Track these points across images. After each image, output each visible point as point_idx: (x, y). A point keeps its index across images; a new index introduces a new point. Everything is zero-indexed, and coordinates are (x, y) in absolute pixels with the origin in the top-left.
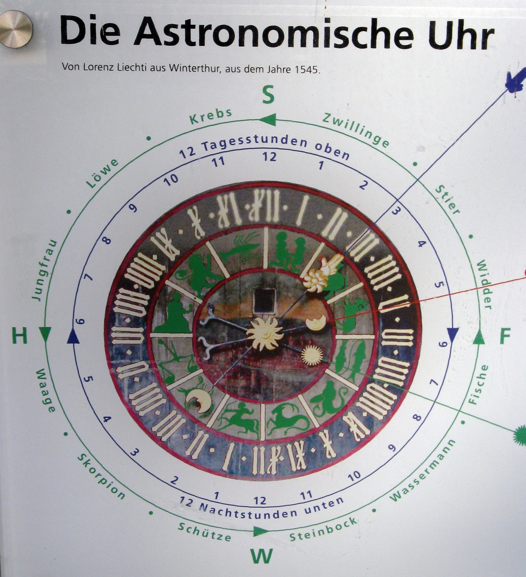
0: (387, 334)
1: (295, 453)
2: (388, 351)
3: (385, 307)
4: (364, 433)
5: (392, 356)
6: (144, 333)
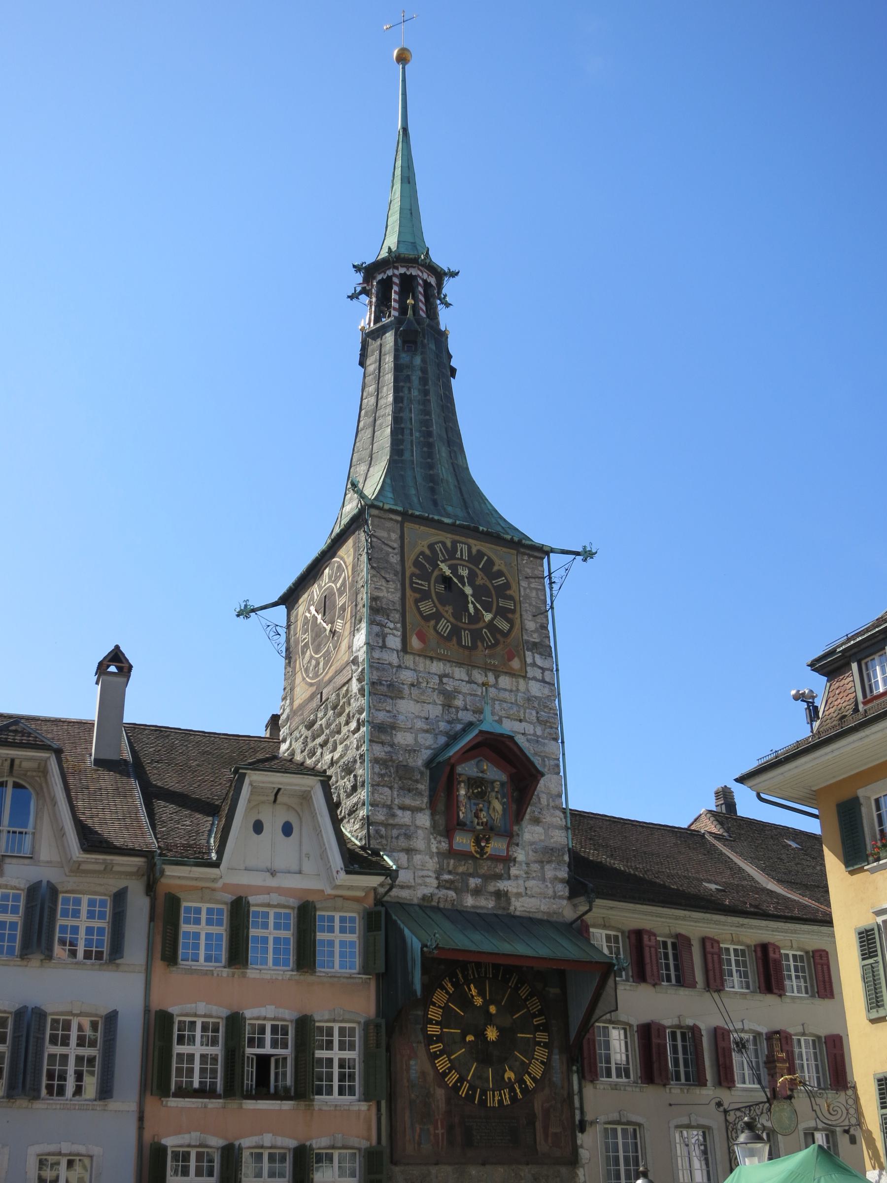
0: (538, 1035)
1: (505, 1095)
2: (539, 1044)
3: (536, 1021)
4: (532, 1085)
5: (541, 1046)
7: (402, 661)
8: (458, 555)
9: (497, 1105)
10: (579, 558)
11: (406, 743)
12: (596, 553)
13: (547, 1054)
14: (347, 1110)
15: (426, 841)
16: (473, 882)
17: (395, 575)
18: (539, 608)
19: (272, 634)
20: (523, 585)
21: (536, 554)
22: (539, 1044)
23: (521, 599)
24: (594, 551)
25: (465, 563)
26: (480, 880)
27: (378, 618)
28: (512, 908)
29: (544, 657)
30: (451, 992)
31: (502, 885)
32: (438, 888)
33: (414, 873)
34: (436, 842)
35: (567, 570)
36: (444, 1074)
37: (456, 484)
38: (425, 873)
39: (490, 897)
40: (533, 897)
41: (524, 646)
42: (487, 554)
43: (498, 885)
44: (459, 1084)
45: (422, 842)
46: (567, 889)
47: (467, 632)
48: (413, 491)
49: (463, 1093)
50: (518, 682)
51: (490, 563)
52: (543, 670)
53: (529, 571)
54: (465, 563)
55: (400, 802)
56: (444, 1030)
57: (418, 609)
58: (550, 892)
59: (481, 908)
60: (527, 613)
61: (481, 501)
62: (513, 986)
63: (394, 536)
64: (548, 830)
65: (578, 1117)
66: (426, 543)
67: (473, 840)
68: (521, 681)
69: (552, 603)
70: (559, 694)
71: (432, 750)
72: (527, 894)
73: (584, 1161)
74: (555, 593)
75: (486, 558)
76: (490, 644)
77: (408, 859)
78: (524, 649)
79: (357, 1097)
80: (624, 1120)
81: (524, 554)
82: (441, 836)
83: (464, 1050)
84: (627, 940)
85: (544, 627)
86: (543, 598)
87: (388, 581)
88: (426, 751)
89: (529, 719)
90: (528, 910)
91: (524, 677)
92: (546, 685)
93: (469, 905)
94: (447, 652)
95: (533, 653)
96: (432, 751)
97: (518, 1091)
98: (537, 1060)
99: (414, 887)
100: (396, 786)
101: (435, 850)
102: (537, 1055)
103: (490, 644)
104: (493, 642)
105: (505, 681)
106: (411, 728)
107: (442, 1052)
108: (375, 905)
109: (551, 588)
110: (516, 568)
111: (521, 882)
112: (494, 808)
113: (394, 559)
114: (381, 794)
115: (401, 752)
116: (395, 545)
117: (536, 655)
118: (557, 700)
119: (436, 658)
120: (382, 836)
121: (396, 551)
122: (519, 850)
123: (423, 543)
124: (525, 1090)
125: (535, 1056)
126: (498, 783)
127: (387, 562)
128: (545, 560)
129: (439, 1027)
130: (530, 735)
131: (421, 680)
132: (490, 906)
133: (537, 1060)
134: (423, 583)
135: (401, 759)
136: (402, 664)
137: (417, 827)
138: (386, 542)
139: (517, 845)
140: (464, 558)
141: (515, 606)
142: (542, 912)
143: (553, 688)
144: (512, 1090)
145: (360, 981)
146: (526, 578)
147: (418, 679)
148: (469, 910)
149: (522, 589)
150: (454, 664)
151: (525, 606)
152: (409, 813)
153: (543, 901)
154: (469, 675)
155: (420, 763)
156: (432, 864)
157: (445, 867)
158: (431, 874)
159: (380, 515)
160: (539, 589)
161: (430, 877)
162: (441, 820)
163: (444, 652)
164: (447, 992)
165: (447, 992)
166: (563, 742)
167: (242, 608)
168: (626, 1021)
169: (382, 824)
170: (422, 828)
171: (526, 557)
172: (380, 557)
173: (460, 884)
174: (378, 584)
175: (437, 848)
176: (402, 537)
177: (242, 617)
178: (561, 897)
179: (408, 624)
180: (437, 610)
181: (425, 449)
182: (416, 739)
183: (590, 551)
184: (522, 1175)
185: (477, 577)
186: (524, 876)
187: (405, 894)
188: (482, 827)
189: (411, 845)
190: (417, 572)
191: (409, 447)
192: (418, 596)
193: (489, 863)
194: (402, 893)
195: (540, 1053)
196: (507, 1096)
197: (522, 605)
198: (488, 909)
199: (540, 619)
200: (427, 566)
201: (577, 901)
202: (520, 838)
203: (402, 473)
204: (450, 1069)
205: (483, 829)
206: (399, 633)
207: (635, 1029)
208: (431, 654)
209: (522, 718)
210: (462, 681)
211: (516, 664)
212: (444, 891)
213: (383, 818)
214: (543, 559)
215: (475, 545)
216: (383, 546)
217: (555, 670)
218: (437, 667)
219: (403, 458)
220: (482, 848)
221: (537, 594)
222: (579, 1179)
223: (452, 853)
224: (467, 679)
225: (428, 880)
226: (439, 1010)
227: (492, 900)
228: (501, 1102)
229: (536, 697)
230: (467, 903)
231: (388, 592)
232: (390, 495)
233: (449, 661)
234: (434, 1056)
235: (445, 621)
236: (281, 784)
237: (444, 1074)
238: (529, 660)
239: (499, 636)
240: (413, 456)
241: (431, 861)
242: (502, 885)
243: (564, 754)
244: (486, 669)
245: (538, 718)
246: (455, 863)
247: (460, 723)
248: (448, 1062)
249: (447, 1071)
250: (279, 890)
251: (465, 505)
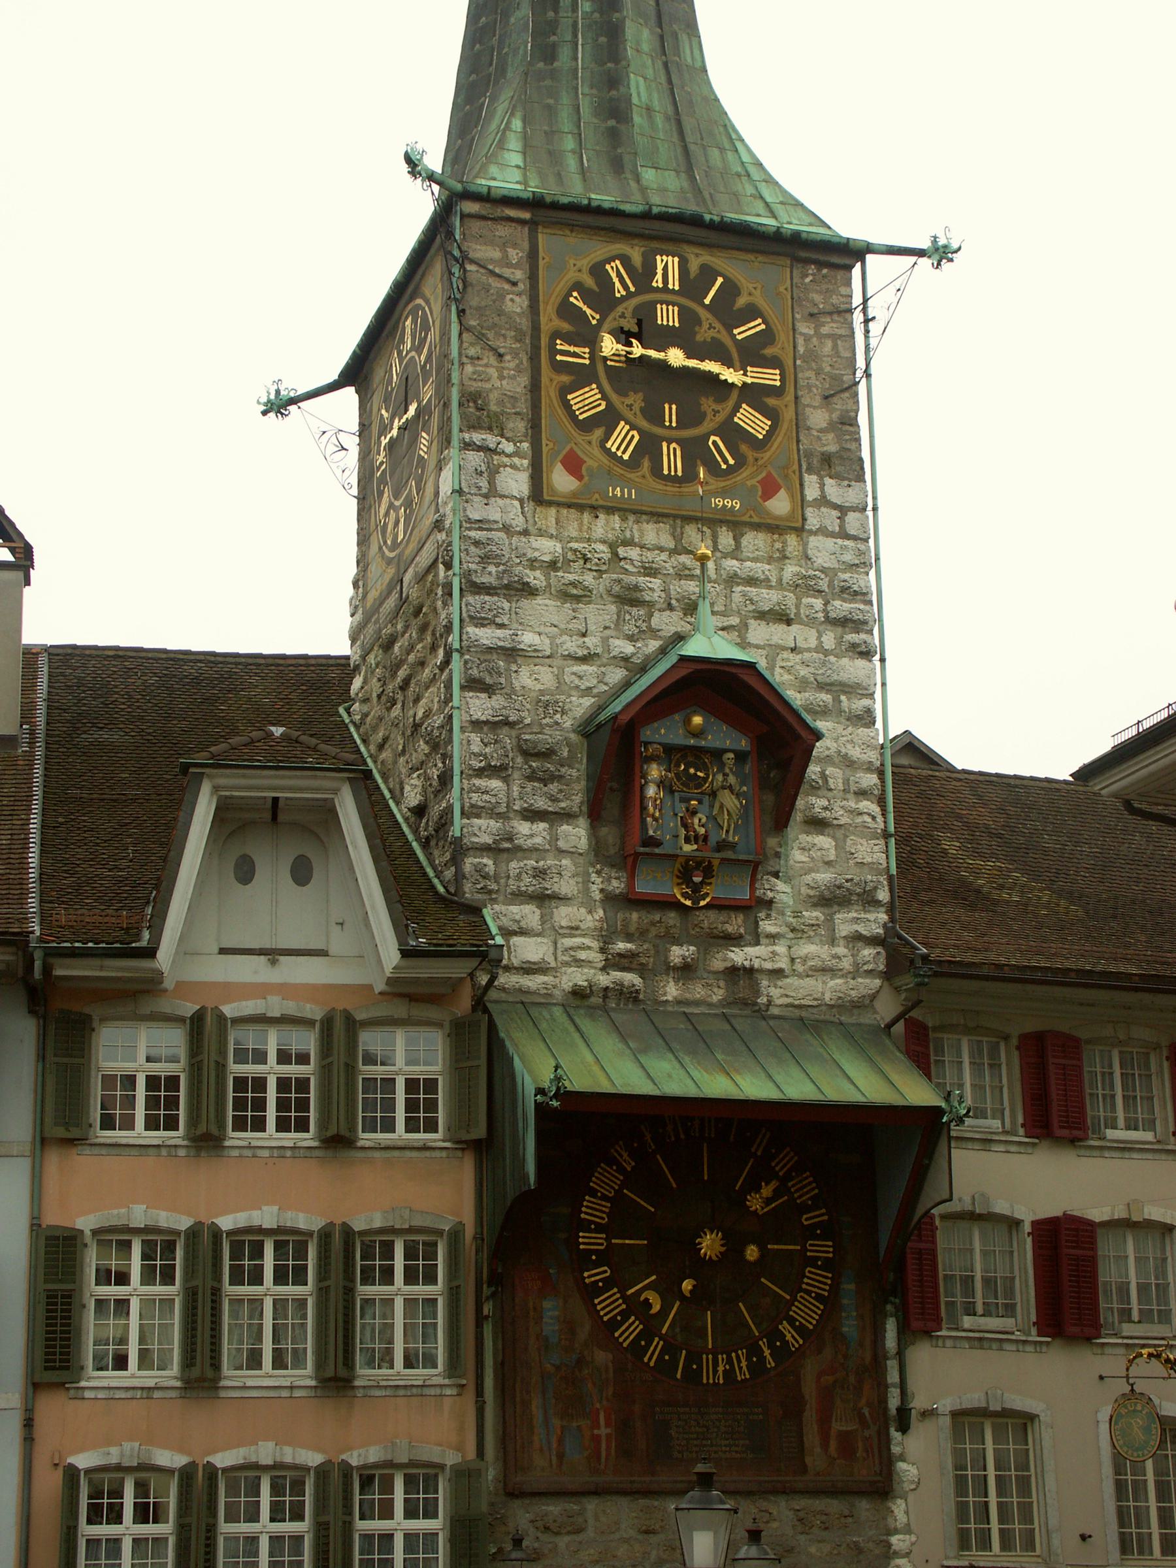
1: (739, 1361)
2: (812, 1262)
3: (807, 1219)
4: (798, 1342)
5: (818, 1268)
6: (605, 1239)
7: (531, 521)
8: (658, 282)
9: (721, 1381)
10: (925, 262)
11: (539, 687)
12: (959, 249)
13: (829, 1282)
14: (417, 1396)
15: (580, 880)
16: (678, 953)
17: (518, 340)
18: (836, 378)
19: (332, 448)
20: (806, 331)
21: (836, 260)
22: (812, 1262)
23: (798, 362)
24: (955, 246)
25: (670, 297)
26: (692, 948)
27: (477, 437)
28: (763, 1000)
29: (846, 483)
31: (739, 956)
32: (603, 969)
33: (555, 943)
34: (601, 880)
35: (899, 290)
36: (614, 1324)
37: (670, 110)
38: (577, 941)
39: (714, 982)
40: (808, 976)
41: (800, 466)
42: (722, 271)
43: (731, 955)
44: (643, 1343)
45: (572, 882)
46: (882, 960)
47: (673, 445)
48: (569, 143)
49: (652, 1356)
50: (784, 543)
51: (730, 290)
52: (843, 510)
53: (817, 298)
54: (670, 297)
55: (526, 805)
56: (613, 1241)
57: (567, 406)
58: (846, 964)
59: (697, 1003)
60: (810, 391)
61: (727, 146)
62: (759, 1153)
63: (514, 255)
64: (845, 841)
65: (894, 1402)
66: (585, 263)
67: (676, 872)
68: (792, 540)
69: (868, 365)
70: (877, 559)
71: (593, 697)
72: (794, 970)
73: (907, 1486)
74: (873, 342)
75: (720, 280)
76: (724, 467)
77: (542, 917)
78: (800, 471)
79: (440, 1367)
80: (995, 1407)
81: (807, 261)
82: (613, 866)
83: (654, 1277)
84: (1016, 1053)
85: (849, 422)
86: (848, 354)
87: (501, 356)
88: (582, 701)
89: (807, 616)
90: (797, 1002)
91: (800, 531)
92: (847, 543)
93: (670, 998)
94: (630, 493)
95: (821, 478)
96: (593, 700)
97: (767, 1352)
98: (808, 1293)
99: (555, 969)
100: (516, 775)
101: (597, 896)
102: (807, 1284)
103: (724, 467)
104: (731, 462)
105: (754, 541)
106: (548, 657)
107: (608, 1283)
108: (474, 1009)
109: (867, 331)
110: (789, 297)
111: (781, 949)
112: (722, 806)
113: (516, 304)
114: (486, 792)
115: (528, 706)
116: (519, 275)
117: (828, 481)
118: (872, 573)
119: (603, 507)
120: (488, 873)
121: (521, 286)
122: (781, 886)
123: (579, 264)
124: (782, 1352)
125: (804, 1286)
126: (731, 755)
127: (500, 313)
128: (856, 271)
129: (604, 1236)
130: (809, 650)
131: (570, 556)
132: (715, 999)
133: (808, 1293)
134: (577, 350)
135: (528, 721)
136: (530, 528)
137: (561, 852)
138: (497, 270)
139: (776, 875)
140: (670, 286)
141: (783, 379)
142: (826, 1005)
143: (862, 547)
144: (755, 1350)
145: (444, 1154)
146: (811, 315)
147: (564, 556)
148: (670, 1009)
149: (800, 341)
150: (644, 517)
151: (807, 375)
152: (542, 825)
153: (832, 983)
154: (678, 538)
155: (568, 723)
156: (591, 919)
157: (619, 927)
158: (587, 941)
159: (484, 213)
160: (841, 336)
161: (589, 948)
162: (608, 833)
163: (622, 492)
164: (621, 1170)
165: (621, 1170)
166: (883, 660)
167: (272, 397)
168: (1007, 1212)
169: (486, 849)
170: (572, 853)
171: (812, 269)
172: (483, 304)
173: (652, 960)
174: (481, 362)
175: (602, 891)
176: (533, 255)
177: (272, 415)
178: (870, 973)
179: (544, 442)
180: (610, 405)
181: (603, 40)
182: (559, 678)
183: (945, 247)
184: (775, 1513)
185: (700, 323)
186: (791, 935)
187: (533, 982)
188: (695, 847)
189: (547, 889)
190: (566, 327)
191: (569, 37)
192: (566, 379)
193: (712, 914)
194: (530, 984)
195: (816, 1280)
196: (744, 1364)
197: (800, 375)
198: (710, 1005)
199: (839, 404)
200: (589, 312)
201: (898, 981)
202: (782, 862)
203: (551, 101)
204: (625, 1315)
205: (697, 850)
206: (526, 462)
207: (1027, 1228)
208: (596, 499)
209: (792, 616)
210: (661, 549)
211: (780, 505)
212: (617, 975)
213: (487, 839)
214: (850, 268)
215: (697, 255)
216: (490, 280)
217: (870, 507)
218: (604, 526)
219: (555, 64)
220: (696, 888)
221: (835, 347)
222: (896, 1520)
223: (630, 901)
224: (672, 545)
225: (583, 955)
226: (604, 1203)
227: (719, 987)
228: (730, 1374)
229: (823, 570)
230: (665, 994)
231: (501, 378)
232: (516, 159)
233: (635, 512)
234: (594, 1291)
235: (627, 427)
236: (274, 789)
237: (614, 1324)
238: (811, 493)
239: (744, 448)
240: (576, 59)
241: (589, 917)
242: (739, 956)
243: (884, 684)
244: (714, 521)
245: (827, 617)
246: (640, 918)
247: (656, 638)
248: (620, 1301)
249: (619, 1318)
250: (283, 989)
251: (688, 164)
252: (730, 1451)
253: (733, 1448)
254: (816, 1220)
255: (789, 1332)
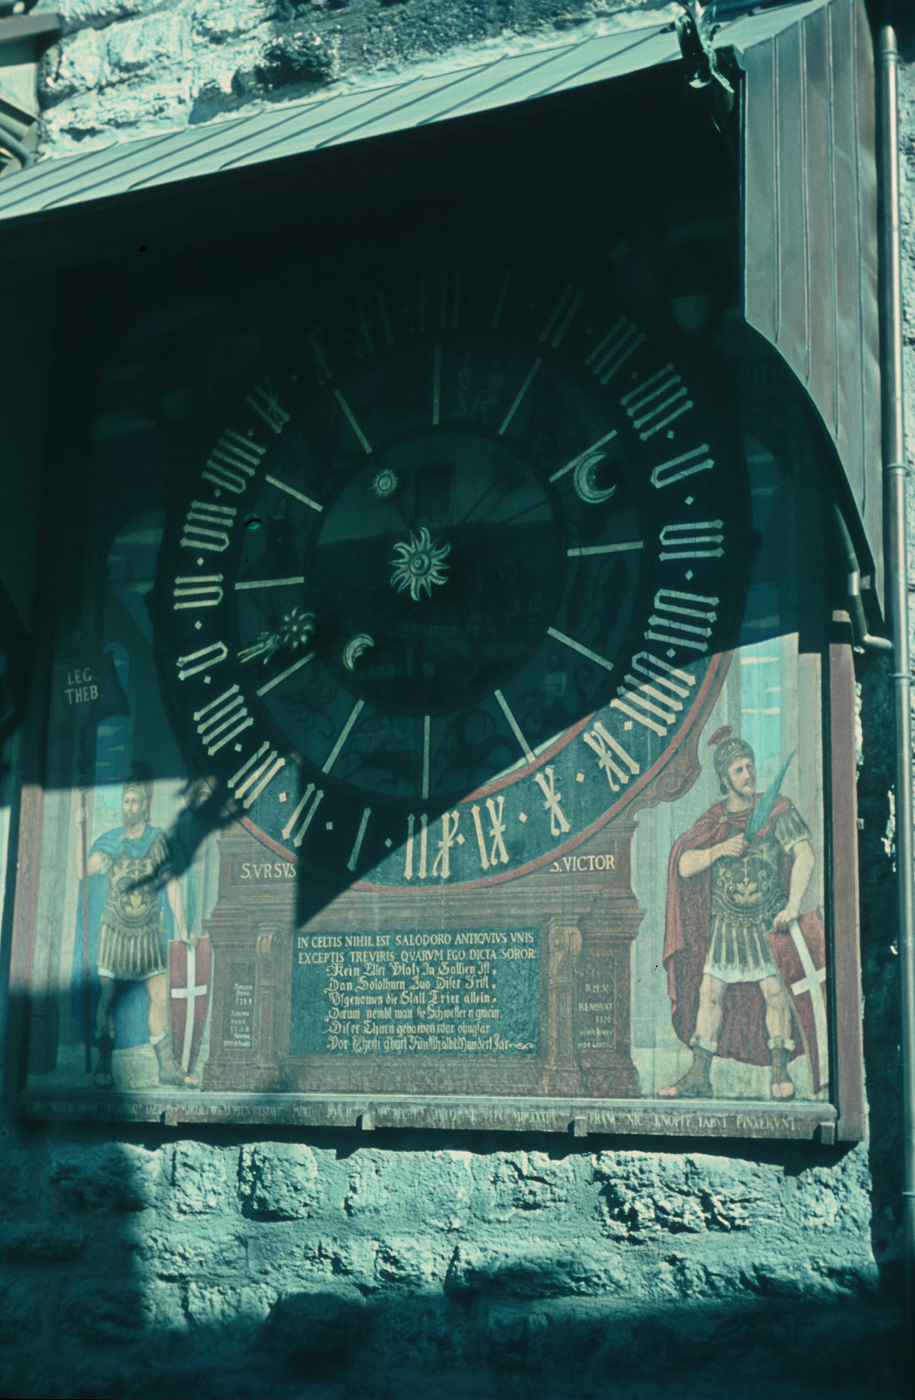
0: (669, 536)
4: (626, 769)
30: (278, 431)
56: (239, 586)
97: (552, 799)
102: (658, 629)
125: (651, 635)
164: (263, 435)
196: (498, 829)
204: (251, 740)
248: (244, 712)
252: (456, 1035)
253: (463, 1028)
254: (685, 473)
255: (608, 748)
